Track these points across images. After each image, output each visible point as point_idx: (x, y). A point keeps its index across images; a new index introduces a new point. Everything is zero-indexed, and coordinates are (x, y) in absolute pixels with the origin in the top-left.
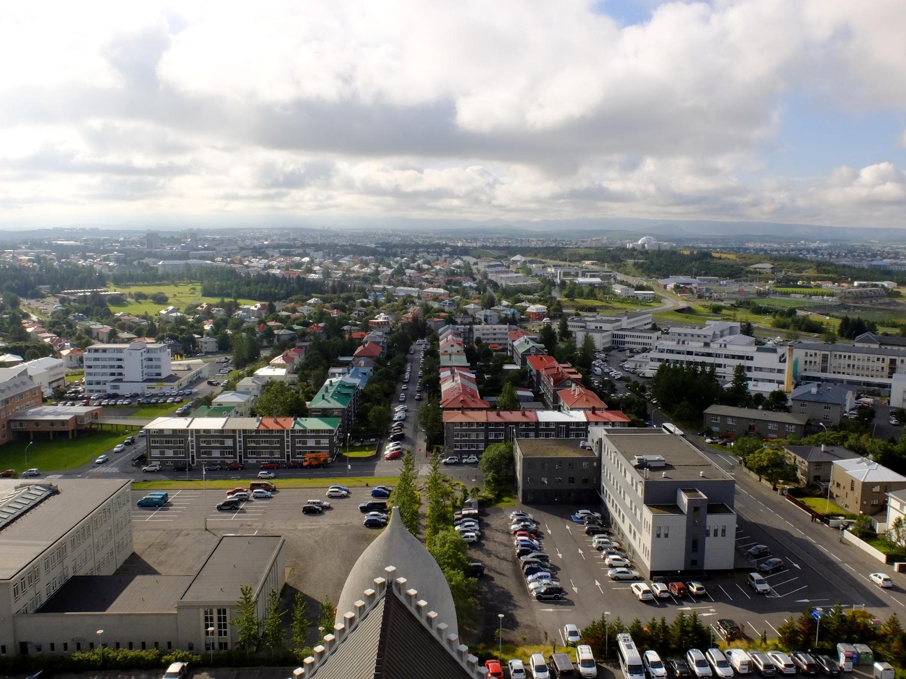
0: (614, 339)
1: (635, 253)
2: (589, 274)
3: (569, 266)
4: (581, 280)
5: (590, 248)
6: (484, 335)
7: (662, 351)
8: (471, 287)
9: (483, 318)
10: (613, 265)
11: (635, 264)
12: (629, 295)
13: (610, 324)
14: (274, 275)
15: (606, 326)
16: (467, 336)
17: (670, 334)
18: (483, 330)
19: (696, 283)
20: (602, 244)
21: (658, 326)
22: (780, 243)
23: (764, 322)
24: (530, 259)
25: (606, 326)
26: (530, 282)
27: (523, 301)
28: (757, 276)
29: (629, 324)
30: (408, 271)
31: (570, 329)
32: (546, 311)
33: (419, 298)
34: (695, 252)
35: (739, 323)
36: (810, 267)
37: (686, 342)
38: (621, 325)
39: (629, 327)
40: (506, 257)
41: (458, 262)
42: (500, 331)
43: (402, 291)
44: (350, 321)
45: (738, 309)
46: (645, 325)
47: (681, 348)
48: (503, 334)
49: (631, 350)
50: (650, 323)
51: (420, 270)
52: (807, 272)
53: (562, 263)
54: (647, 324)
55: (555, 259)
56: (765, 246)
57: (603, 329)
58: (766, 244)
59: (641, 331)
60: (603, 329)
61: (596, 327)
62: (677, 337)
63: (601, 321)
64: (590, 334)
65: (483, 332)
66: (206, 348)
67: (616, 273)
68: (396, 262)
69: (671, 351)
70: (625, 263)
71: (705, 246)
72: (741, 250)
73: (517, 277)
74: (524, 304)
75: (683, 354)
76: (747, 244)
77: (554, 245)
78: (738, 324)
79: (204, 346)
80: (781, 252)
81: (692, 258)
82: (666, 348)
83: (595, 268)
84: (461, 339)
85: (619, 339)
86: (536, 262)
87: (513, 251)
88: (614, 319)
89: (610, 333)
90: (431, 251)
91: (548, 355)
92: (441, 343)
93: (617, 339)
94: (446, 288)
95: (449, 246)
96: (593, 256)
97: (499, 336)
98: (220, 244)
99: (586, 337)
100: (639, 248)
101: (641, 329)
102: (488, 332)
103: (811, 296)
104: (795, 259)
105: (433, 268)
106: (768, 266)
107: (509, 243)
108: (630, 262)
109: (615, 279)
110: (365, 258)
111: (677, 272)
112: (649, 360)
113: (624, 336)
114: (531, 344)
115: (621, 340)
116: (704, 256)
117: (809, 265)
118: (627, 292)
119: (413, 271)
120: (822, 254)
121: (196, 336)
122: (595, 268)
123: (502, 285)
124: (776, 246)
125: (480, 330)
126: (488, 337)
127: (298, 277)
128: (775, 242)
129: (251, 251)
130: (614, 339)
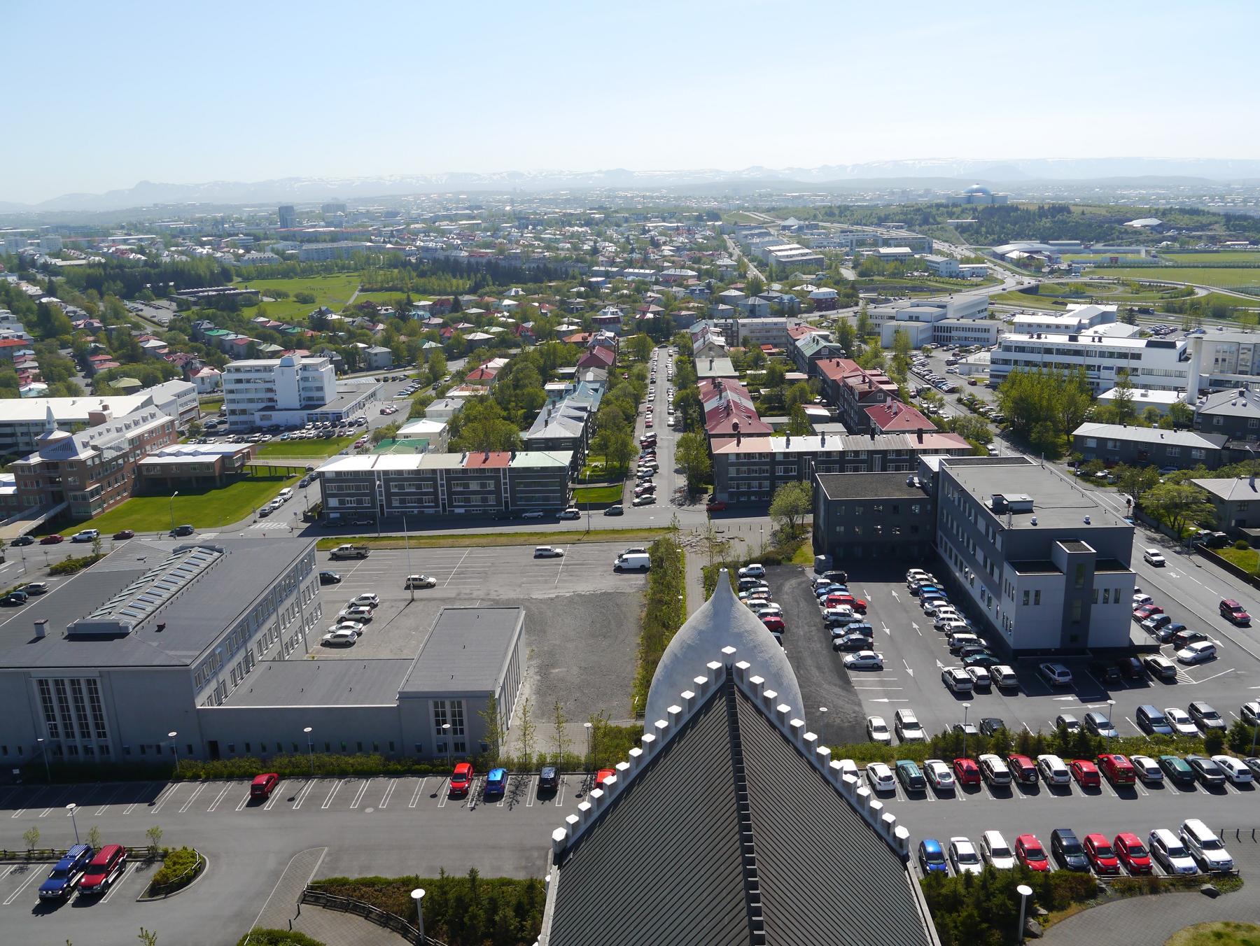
7: (1008, 349)
36: (1216, 223)
37: (1043, 336)
42: (775, 327)
54: (982, 311)
66: (376, 361)
70: (943, 225)
77: (839, 204)
81: (1042, 212)
84: (723, 339)
93: (940, 334)
94: (692, 269)
97: (775, 333)
111: (1018, 236)
114: (823, 343)
115: (946, 334)
116: (1059, 210)
117: (1215, 219)
118: (949, 265)
120: (1233, 201)
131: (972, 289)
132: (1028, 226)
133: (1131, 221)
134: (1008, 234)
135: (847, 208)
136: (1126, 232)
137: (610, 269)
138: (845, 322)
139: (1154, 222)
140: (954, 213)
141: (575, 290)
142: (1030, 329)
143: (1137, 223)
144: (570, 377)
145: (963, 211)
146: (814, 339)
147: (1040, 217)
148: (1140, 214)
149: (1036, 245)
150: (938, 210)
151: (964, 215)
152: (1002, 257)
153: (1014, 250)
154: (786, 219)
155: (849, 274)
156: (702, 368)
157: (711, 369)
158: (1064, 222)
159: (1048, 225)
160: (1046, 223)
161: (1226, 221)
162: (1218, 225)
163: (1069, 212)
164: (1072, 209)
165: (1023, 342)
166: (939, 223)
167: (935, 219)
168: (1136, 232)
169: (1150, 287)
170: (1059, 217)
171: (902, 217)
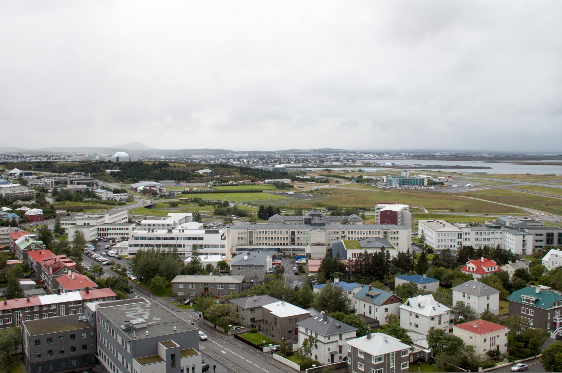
0: (100, 232)
1: (111, 165)
2: (76, 182)
3: (59, 176)
4: (69, 187)
5: (76, 161)
7: (137, 238)
10: (94, 174)
12: (109, 197)
13: (95, 221)
15: (92, 223)
17: (142, 225)
19: (157, 185)
20: (85, 158)
21: (133, 220)
22: (215, 155)
23: (207, 211)
25: (92, 223)
26: (26, 190)
27: (21, 207)
28: (201, 179)
29: (110, 219)
31: (62, 226)
32: (42, 213)
34: (157, 163)
35: (192, 214)
36: (236, 171)
37: (155, 231)
38: (104, 221)
39: (111, 221)
40: (4, 171)
45: (190, 203)
46: (123, 219)
47: (151, 234)
48: (5, 235)
49: (114, 240)
50: (126, 218)
53: (54, 174)
54: (124, 218)
55: (47, 171)
56: (205, 157)
57: (90, 225)
58: (206, 155)
60: (90, 225)
61: (85, 224)
62: (148, 227)
63: (89, 218)
69: (144, 238)
70: (103, 172)
71: (163, 157)
72: (189, 160)
73: (15, 187)
74: (22, 209)
75: (153, 239)
77: (45, 160)
78: (191, 214)
80: (216, 161)
82: (140, 236)
83: (81, 177)
85: (103, 232)
87: (11, 166)
88: (98, 216)
89: (96, 227)
91: (46, 249)
93: (101, 232)
96: (78, 168)
99: (77, 232)
101: (120, 222)
104: (226, 166)
106: (209, 171)
107: (7, 159)
108: (108, 171)
109: (97, 185)
111: (144, 178)
112: (128, 246)
113: (107, 229)
114: (31, 241)
115: (105, 232)
116: (164, 164)
117: (235, 170)
118: (107, 194)
120: (243, 161)
122: (81, 177)
124: (212, 156)
128: (212, 154)
130: (100, 232)
131: (121, 206)
132: (148, 173)
133: (198, 170)
134: (138, 177)
135: (49, 163)
136: (196, 176)
138: (46, 228)
139: (209, 171)
140: (109, 166)
142: (149, 227)
143: (201, 172)
145: (114, 165)
146: (26, 239)
148: (202, 167)
149: (153, 183)
150: (101, 164)
151: (115, 167)
152: (136, 189)
153: (141, 186)
154: (12, 169)
155: (50, 200)
158: (167, 171)
159: (158, 172)
160: (157, 172)
161: (240, 171)
162: (237, 172)
163: (168, 166)
164: (170, 164)
165: (144, 234)
166: (101, 171)
167: (99, 169)
168: (201, 176)
169: (209, 203)
171: (81, 168)
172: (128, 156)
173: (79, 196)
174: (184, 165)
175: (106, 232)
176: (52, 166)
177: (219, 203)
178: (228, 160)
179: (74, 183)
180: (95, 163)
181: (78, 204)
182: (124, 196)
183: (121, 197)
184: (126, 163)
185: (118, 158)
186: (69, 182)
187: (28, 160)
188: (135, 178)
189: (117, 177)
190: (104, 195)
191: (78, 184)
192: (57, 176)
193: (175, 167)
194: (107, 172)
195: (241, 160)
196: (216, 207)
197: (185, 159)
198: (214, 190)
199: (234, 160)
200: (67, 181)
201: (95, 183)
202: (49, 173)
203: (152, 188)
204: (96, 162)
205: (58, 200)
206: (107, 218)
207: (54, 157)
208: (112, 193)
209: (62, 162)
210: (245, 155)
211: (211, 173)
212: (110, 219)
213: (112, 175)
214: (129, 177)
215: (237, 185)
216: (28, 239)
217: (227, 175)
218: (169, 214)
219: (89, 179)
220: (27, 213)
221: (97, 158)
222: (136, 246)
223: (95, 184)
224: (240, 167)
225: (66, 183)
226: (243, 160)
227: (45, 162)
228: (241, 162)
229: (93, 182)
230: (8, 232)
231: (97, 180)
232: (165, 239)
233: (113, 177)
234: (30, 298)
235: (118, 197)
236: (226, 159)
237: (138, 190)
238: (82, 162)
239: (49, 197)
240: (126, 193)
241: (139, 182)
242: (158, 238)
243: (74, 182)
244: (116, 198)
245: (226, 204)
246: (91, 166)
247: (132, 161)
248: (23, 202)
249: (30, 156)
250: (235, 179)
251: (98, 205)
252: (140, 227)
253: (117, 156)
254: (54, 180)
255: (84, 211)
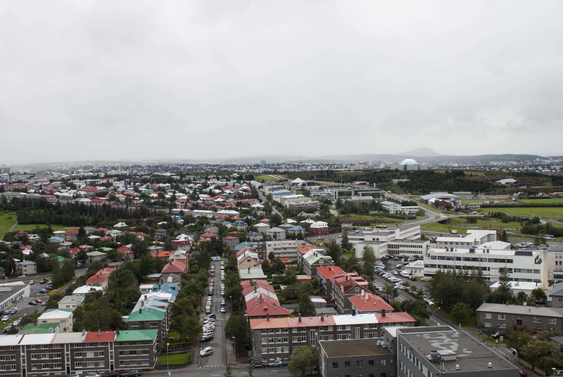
0: (390, 249)
1: (398, 173)
2: (360, 193)
3: (343, 186)
4: (354, 198)
5: (360, 170)
6: (275, 249)
7: (434, 258)
8: (258, 208)
9: (272, 235)
10: (380, 184)
11: (399, 183)
12: (397, 210)
13: (385, 237)
14: (82, 203)
15: (381, 238)
16: (261, 250)
17: (438, 243)
18: (275, 245)
19: (452, 196)
20: (369, 167)
21: (426, 237)
22: (518, 161)
23: (512, 228)
24: (308, 181)
25: (381, 238)
26: (309, 202)
27: (306, 219)
28: (503, 190)
29: (401, 235)
30: (202, 196)
31: (350, 241)
32: (327, 226)
33: (213, 219)
34: (450, 172)
35: (495, 231)
36: (547, 181)
37: (454, 250)
39: (402, 238)
40: (287, 180)
41: (245, 187)
42: (290, 246)
43: (197, 213)
44: (154, 242)
45: (491, 219)
46: (415, 235)
47: (450, 254)
48: (292, 248)
49: (406, 259)
50: (419, 234)
51: (212, 194)
52: (545, 185)
53: (336, 184)
54: (417, 235)
56: (507, 164)
57: (380, 240)
58: (507, 162)
59: (412, 241)
60: (380, 240)
61: (374, 239)
62: (444, 245)
64: (370, 245)
65: (275, 247)
66: (26, 271)
67: (384, 191)
68: (191, 188)
69: (442, 258)
70: (390, 182)
71: (456, 165)
72: (487, 168)
73: (298, 198)
74: (307, 221)
75: (452, 260)
76: (491, 163)
77: (326, 169)
78: (494, 232)
79: (24, 268)
80: (520, 169)
82: (437, 255)
83: (366, 188)
84: (257, 254)
85: (394, 249)
86: (313, 184)
87: (293, 176)
89: (386, 244)
90: (221, 177)
92: (239, 259)
93: (392, 249)
94: (237, 210)
95: (236, 172)
96: (362, 178)
97: (289, 250)
98: (31, 177)
100: (402, 169)
101: (412, 239)
102: (279, 247)
103: (347, 230)
104: (533, 174)
105: (223, 192)
106: (512, 181)
107: (288, 169)
108: (395, 181)
109: (383, 196)
110: (161, 185)
112: (423, 267)
113: (398, 246)
114: (320, 256)
115: (396, 249)
116: (458, 173)
117: (545, 179)
118: (395, 207)
119: (206, 196)
120: (555, 169)
121: (16, 260)
122: (366, 188)
123: (286, 206)
124: (515, 163)
125: (270, 247)
126: (279, 251)
127: (104, 205)
128: (515, 161)
129: (60, 182)
130: (390, 249)
134: (429, 188)
135: (332, 172)
137: (183, 210)
138: (334, 243)
139: (512, 181)
140: (396, 175)
141: (160, 223)
142: (446, 246)
143: (503, 182)
144: (157, 280)
145: (401, 174)
147: (447, 178)
148: (504, 176)
149: (446, 195)
150: (386, 173)
151: (402, 176)
152: (426, 202)
153: (432, 198)
154: (295, 179)
155: (334, 212)
156: (243, 273)
157: (249, 273)
158: (462, 181)
159: (452, 182)
160: (450, 181)
161: (553, 180)
162: (548, 182)
163: (464, 175)
164: (465, 173)
165: (442, 253)
166: (387, 181)
167: (385, 178)
168: (503, 186)
169: (514, 219)
170: (458, 178)
171: (365, 178)
172: (418, 164)
173: (364, 208)
174: (483, 174)
175: (397, 249)
176: (335, 175)
177: (526, 219)
178: (535, 167)
179: (359, 194)
180: (380, 172)
181: (364, 217)
182: (414, 209)
183: (410, 210)
184: (415, 172)
185: (405, 166)
186: (353, 193)
187: (309, 169)
188: (426, 189)
189: (405, 188)
190: (392, 208)
191: (363, 195)
192: (340, 187)
193: (471, 175)
194: (394, 182)
195: (553, 167)
196: (524, 223)
197: (483, 166)
198: (520, 204)
199: (544, 168)
200: (351, 191)
201: (381, 194)
202: (333, 184)
203: (446, 201)
204: (382, 171)
205: (343, 213)
206: (398, 234)
207: (335, 166)
208: (400, 205)
209: (345, 171)
210: (557, 161)
211: (515, 183)
212: (401, 235)
213: (400, 185)
214: (418, 188)
215: (549, 198)
216: (317, 254)
217: (535, 186)
218: (468, 231)
219: (375, 189)
220: (312, 226)
221: (382, 166)
222: (433, 266)
223: (381, 195)
224: (552, 176)
225: (349, 194)
226: (554, 167)
227: (327, 171)
228: (552, 169)
229: (379, 193)
230: (296, 246)
231: (383, 191)
232: (467, 259)
233: (401, 187)
234: (301, 318)
235: (407, 210)
236: (533, 166)
237: (429, 202)
238: (367, 171)
239: (333, 209)
240: (416, 206)
241: (429, 194)
242: (459, 259)
243: (359, 193)
244: (405, 211)
245: (536, 221)
246: (376, 175)
247: (422, 169)
248: (308, 214)
249: (311, 164)
250: (546, 191)
251: (386, 219)
252: (435, 244)
253: (405, 164)
254: (337, 190)
255: (371, 225)
